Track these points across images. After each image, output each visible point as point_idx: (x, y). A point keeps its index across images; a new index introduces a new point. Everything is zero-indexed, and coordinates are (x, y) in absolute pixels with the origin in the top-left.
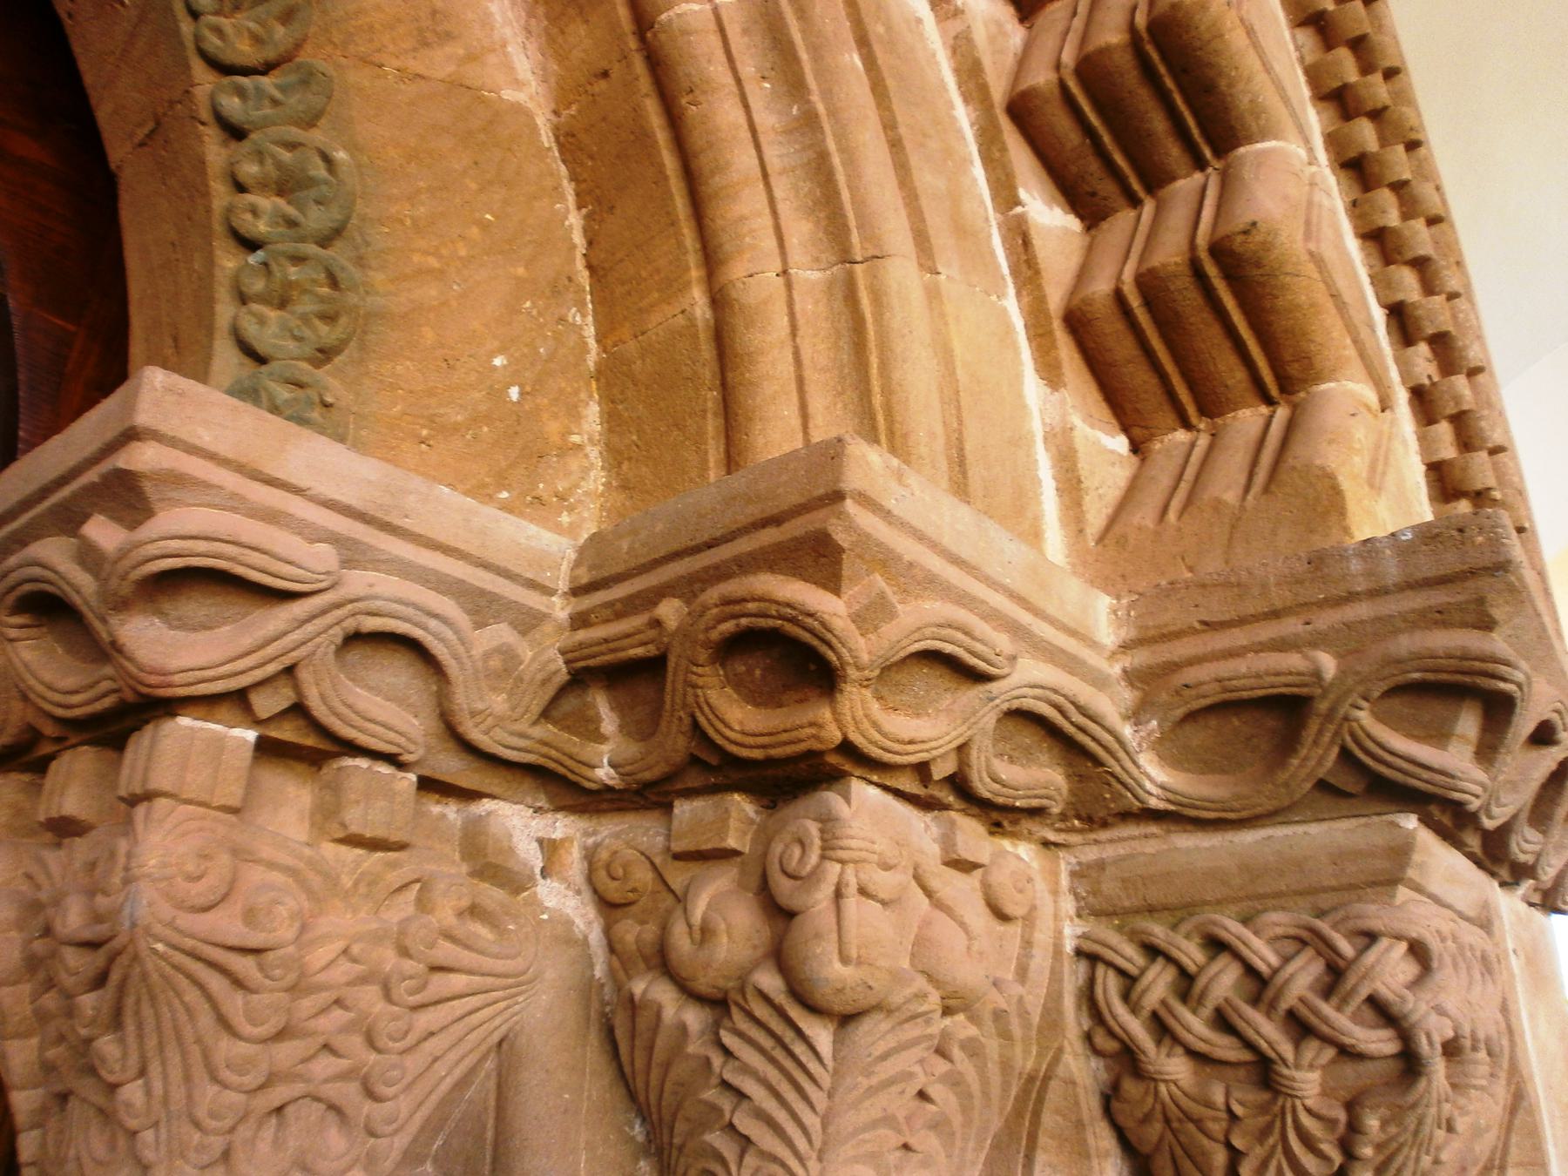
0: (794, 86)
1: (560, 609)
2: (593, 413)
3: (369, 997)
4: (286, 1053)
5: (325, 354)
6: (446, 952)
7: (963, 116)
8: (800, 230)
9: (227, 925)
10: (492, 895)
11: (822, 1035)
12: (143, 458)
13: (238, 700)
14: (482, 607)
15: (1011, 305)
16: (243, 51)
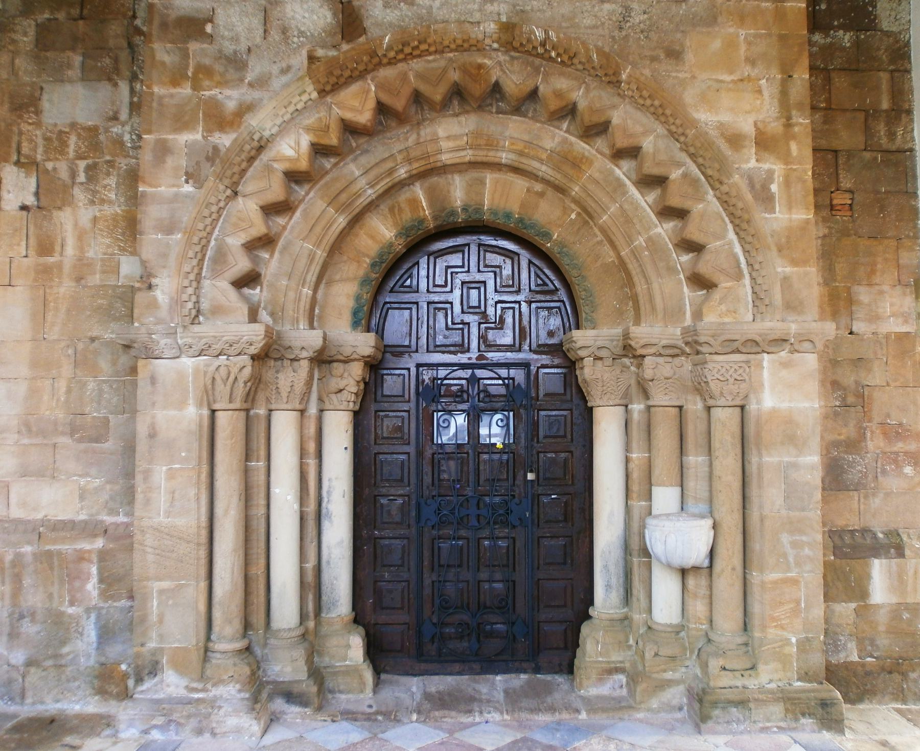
0: (638, 261)
1: (622, 338)
2: (631, 303)
3: (612, 382)
4: (605, 388)
5: (593, 312)
6: (619, 376)
7: (671, 246)
8: (643, 281)
9: (594, 377)
10: (625, 369)
11: (650, 383)
12: (574, 339)
13: (590, 356)
14: (612, 341)
15: (682, 276)
16: (576, 275)
